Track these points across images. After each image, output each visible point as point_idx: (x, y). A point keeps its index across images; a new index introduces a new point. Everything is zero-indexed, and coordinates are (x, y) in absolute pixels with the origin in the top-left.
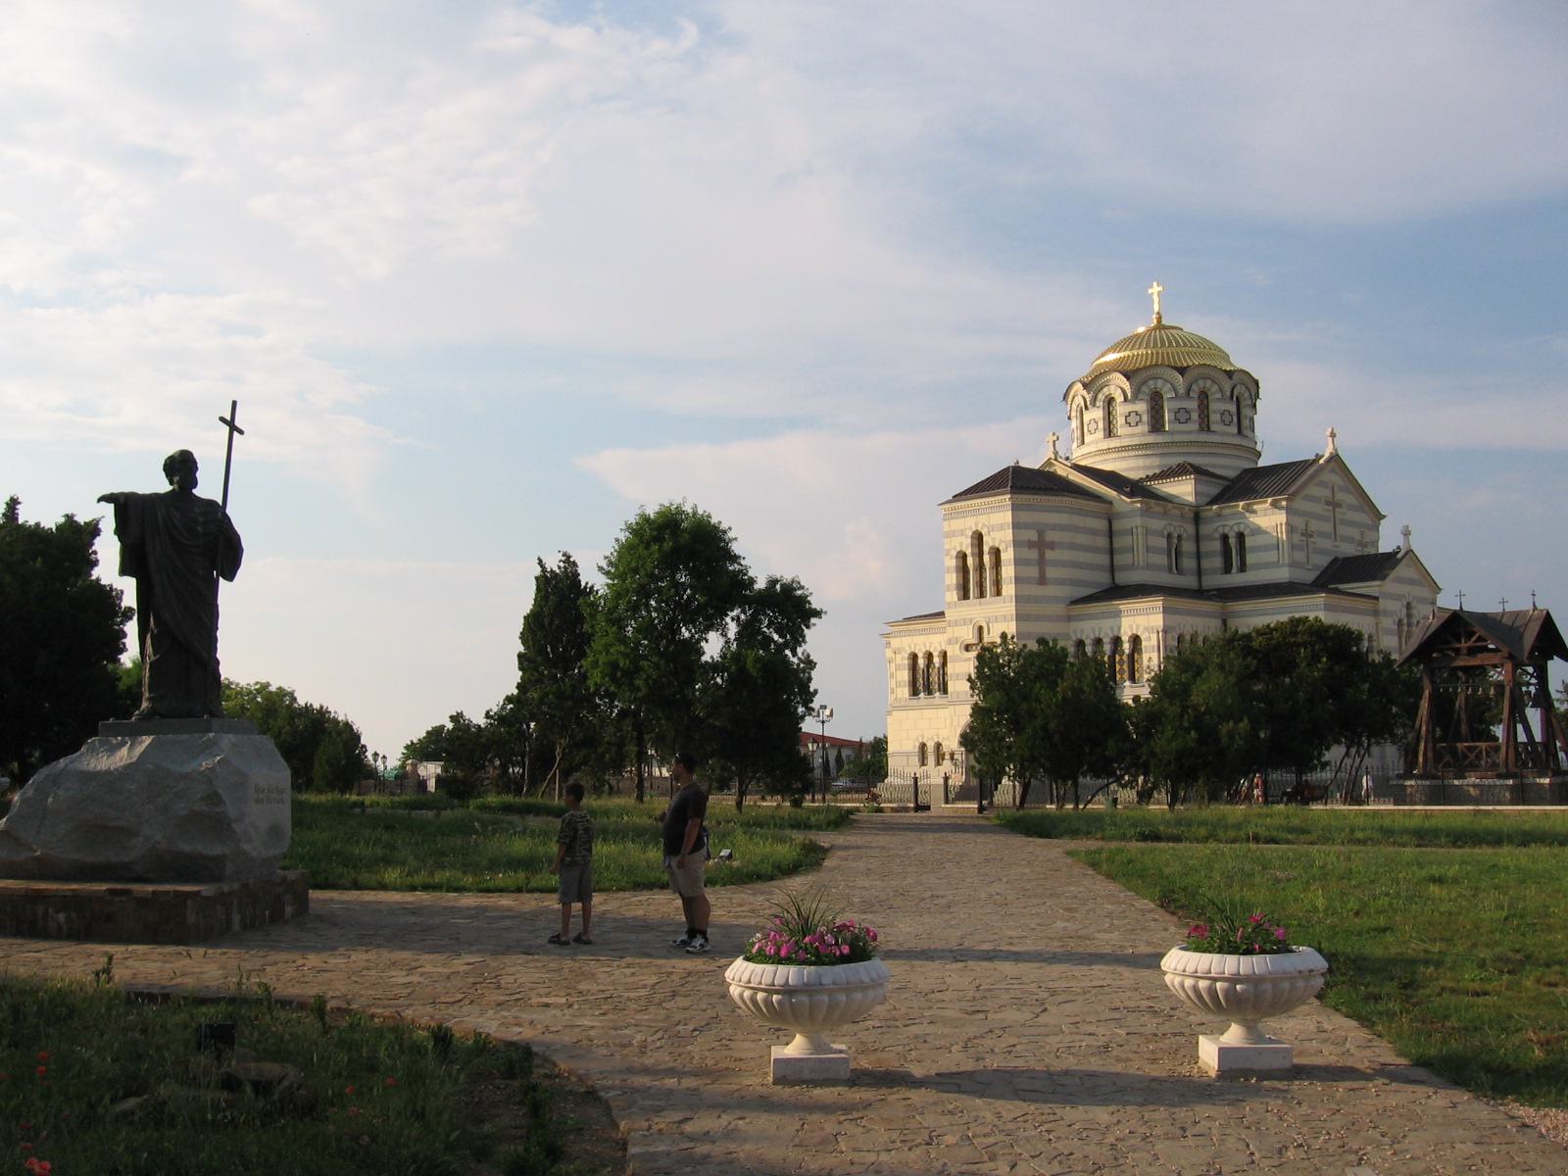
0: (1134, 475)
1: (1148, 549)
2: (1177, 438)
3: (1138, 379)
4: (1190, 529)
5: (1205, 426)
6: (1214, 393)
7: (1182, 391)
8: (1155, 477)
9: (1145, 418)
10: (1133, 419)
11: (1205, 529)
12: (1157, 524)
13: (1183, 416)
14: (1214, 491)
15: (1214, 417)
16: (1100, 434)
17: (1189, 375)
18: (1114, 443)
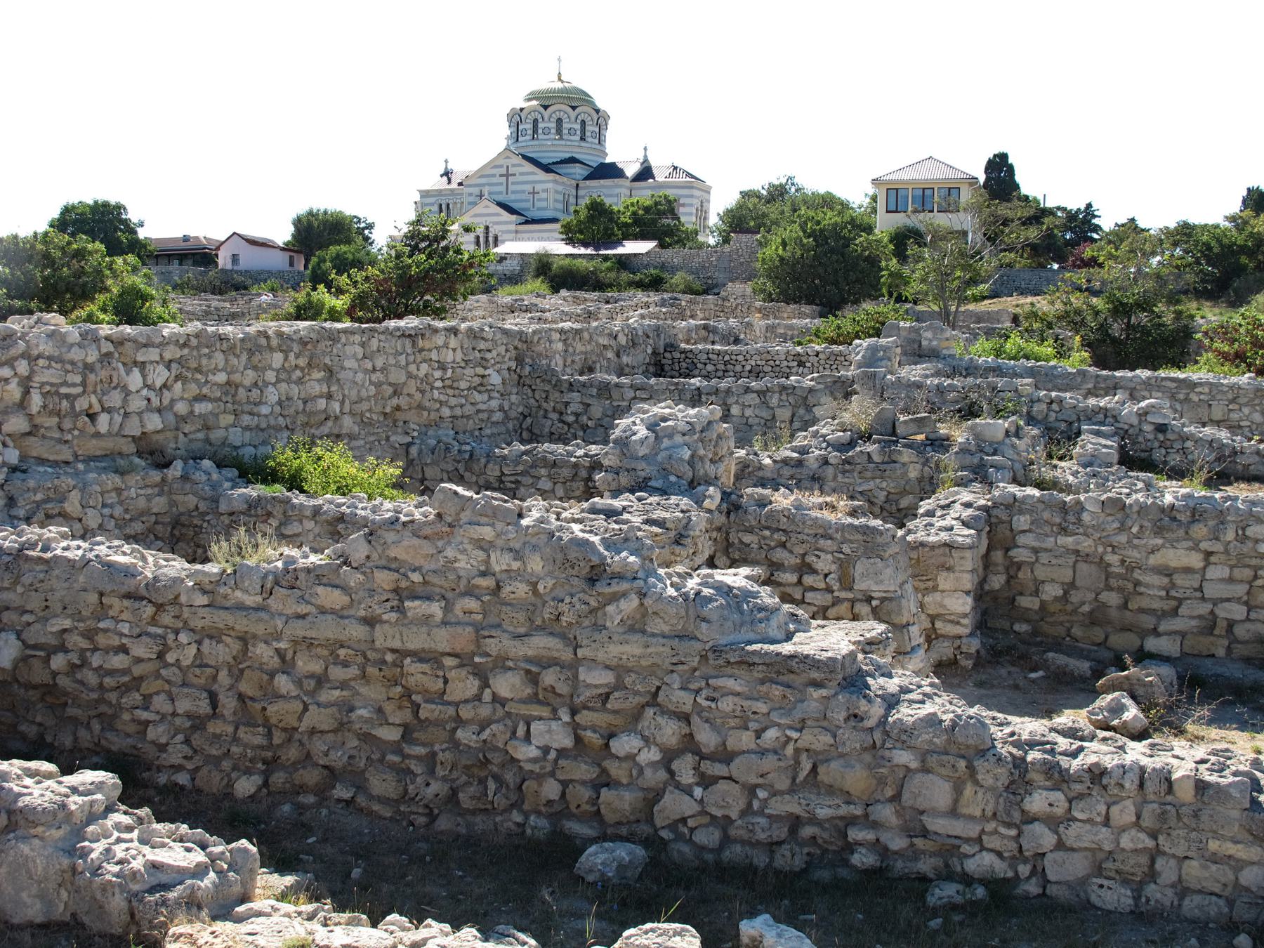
0: (545, 161)
1: (556, 201)
3: (550, 110)
4: (574, 192)
5: (583, 139)
6: (588, 122)
7: (573, 119)
8: (557, 163)
9: (553, 131)
10: (546, 131)
11: (581, 193)
12: (560, 188)
14: (586, 173)
15: (588, 134)
16: (528, 138)
17: (578, 110)
18: (535, 143)
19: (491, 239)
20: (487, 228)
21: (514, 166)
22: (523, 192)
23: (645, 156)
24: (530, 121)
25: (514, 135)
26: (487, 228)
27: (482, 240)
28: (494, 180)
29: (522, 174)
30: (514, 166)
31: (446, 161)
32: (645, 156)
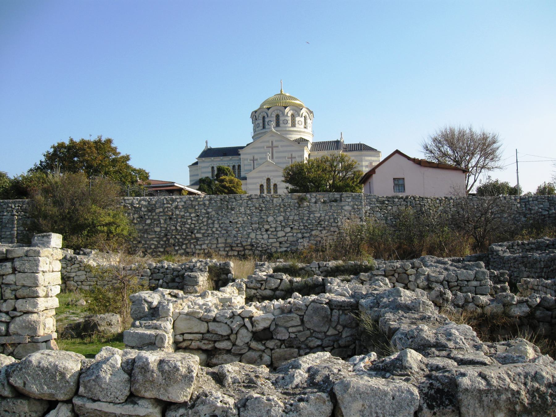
2: (299, 130)
9: (290, 122)
10: (285, 122)
13: (300, 123)
19: (272, 187)
20: (268, 180)
21: (277, 141)
22: (285, 157)
23: (341, 138)
24: (274, 115)
25: (261, 125)
26: (268, 180)
27: (265, 187)
28: (262, 150)
29: (282, 146)
30: (277, 141)
31: (207, 142)
32: (341, 138)
